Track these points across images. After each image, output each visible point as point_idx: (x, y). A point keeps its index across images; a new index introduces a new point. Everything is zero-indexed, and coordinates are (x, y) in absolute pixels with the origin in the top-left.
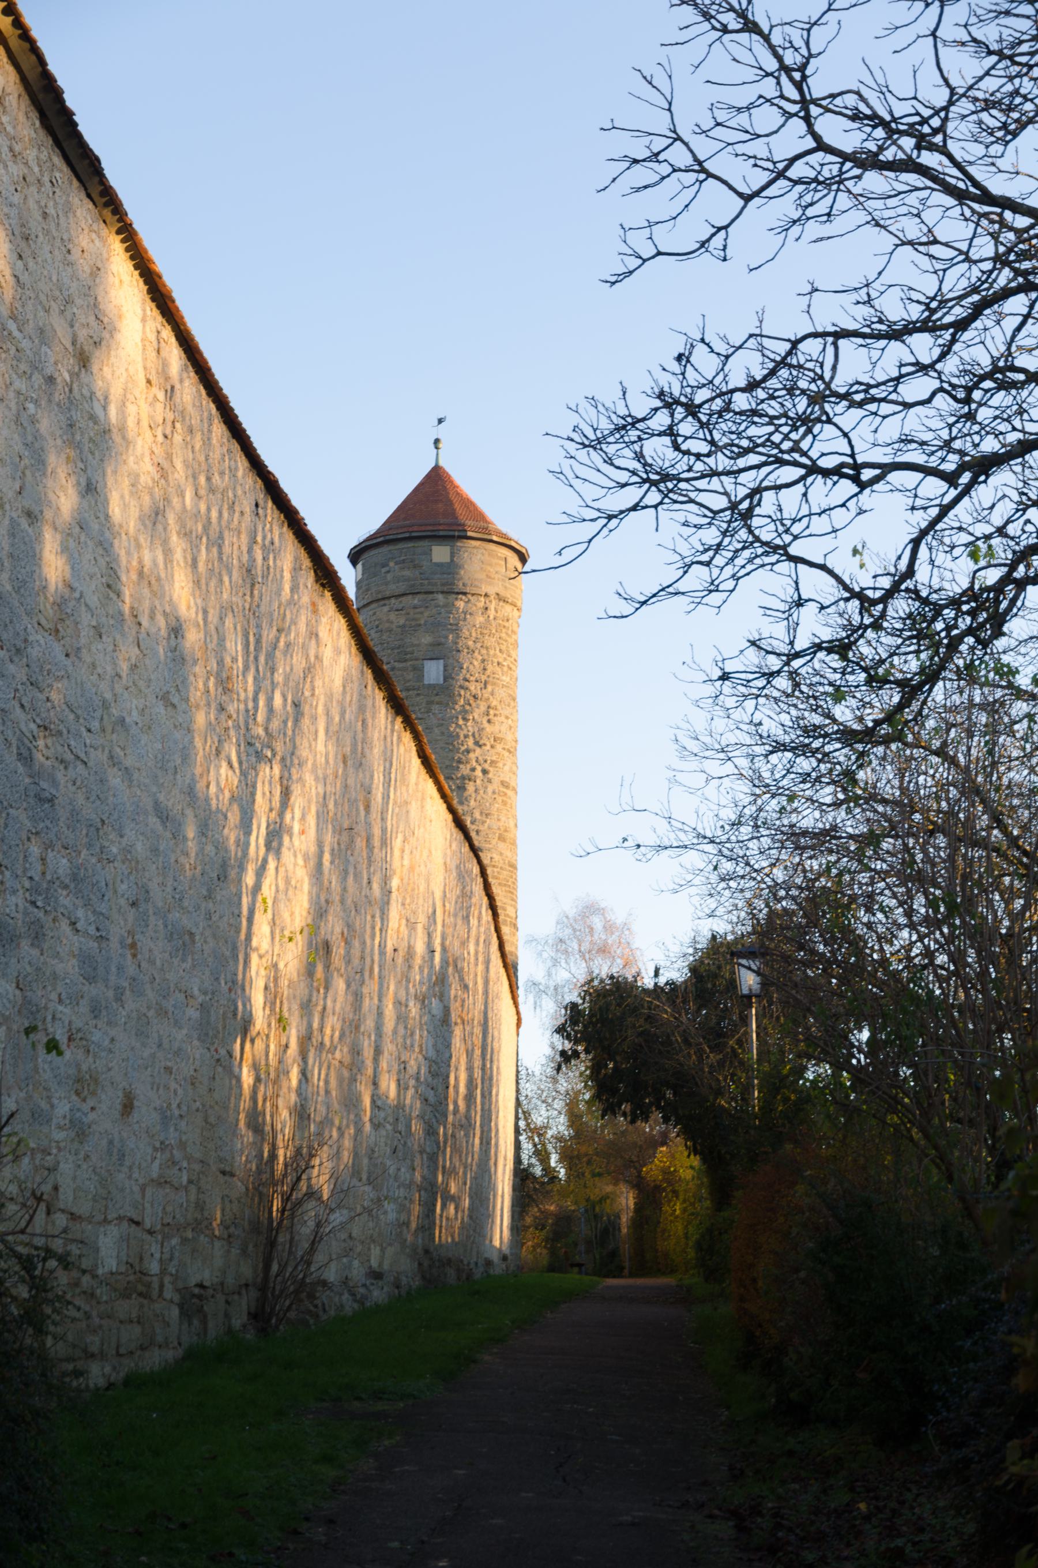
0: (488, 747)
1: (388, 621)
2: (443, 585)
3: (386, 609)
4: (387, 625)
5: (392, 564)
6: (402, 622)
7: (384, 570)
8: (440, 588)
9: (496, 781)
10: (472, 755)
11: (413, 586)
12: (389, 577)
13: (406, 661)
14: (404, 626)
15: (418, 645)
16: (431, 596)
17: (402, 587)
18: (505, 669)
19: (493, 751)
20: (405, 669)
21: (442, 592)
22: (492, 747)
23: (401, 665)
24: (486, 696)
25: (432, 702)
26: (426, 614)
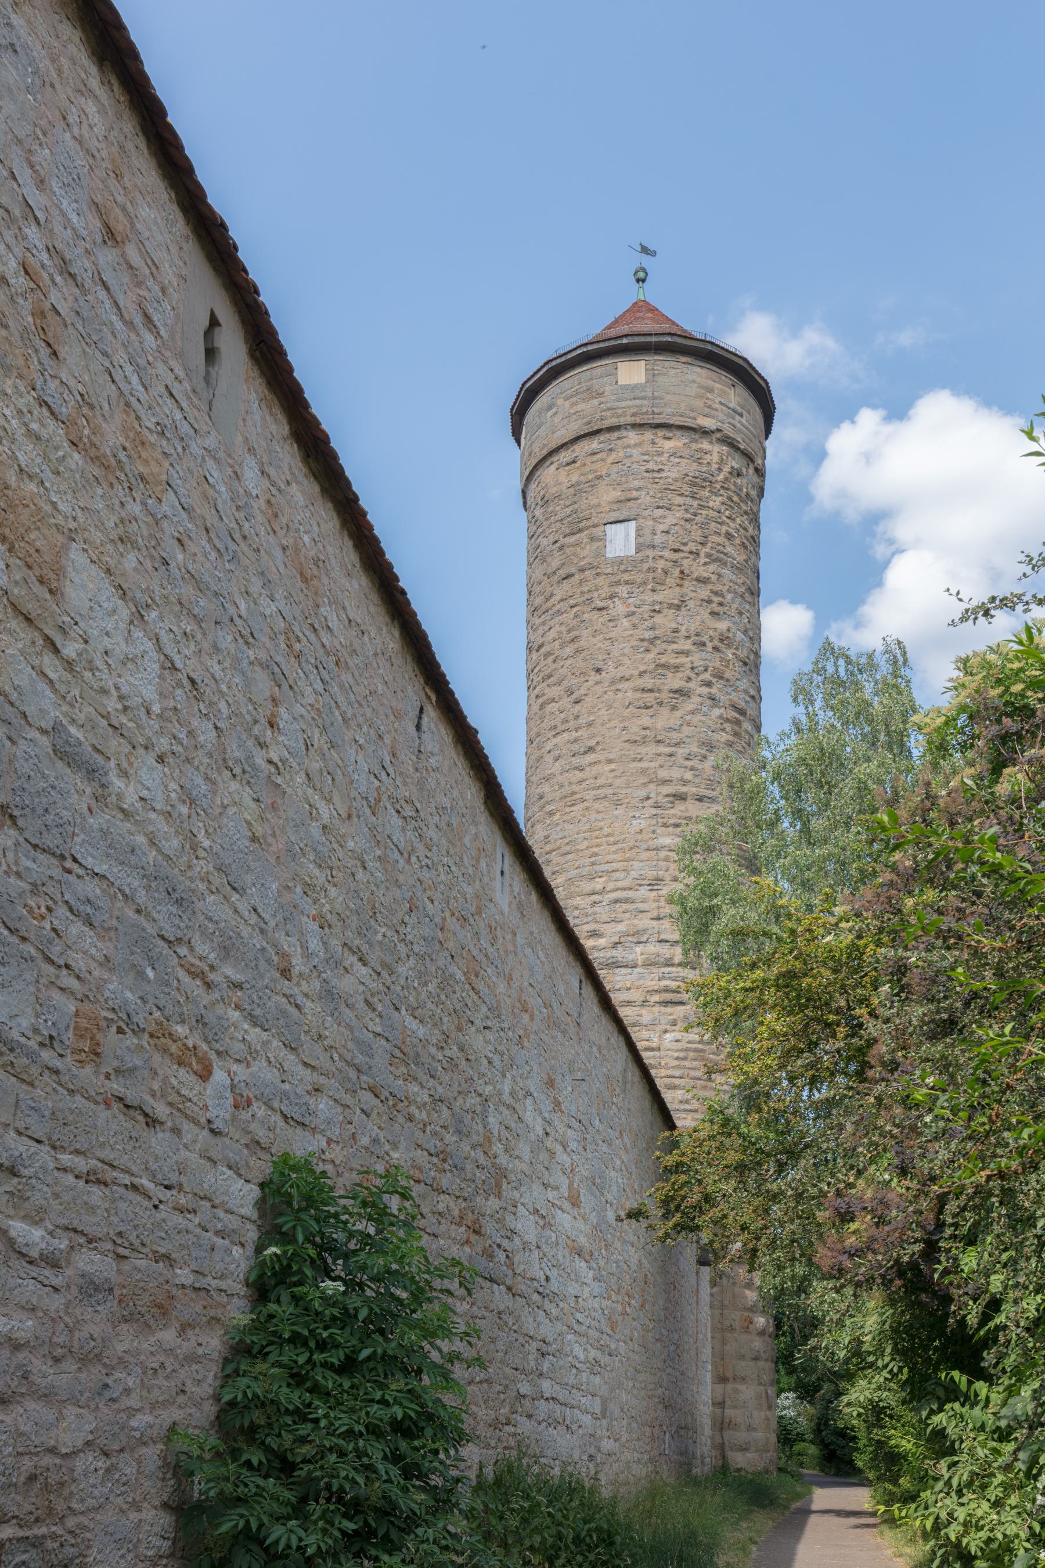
0: (710, 645)
1: (558, 483)
2: (634, 415)
3: (553, 468)
4: (553, 490)
5: (560, 402)
6: (575, 478)
7: (550, 413)
8: (630, 420)
9: (723, 699)
10: (682, 659)
11: (589, 423)
12: (556, 420)
13: (580, 531)
14: (578, 483)
15: (599, 505)
16: (616, 434)
17: (575, 428)
18: (738, 541)
19: (718, 655)
20: (578, 544)
21: (634, 426)
22: (716, 649)
23: (573, 539)
24: (705, 575)
25: (618, 583)
26: (610, 460)
